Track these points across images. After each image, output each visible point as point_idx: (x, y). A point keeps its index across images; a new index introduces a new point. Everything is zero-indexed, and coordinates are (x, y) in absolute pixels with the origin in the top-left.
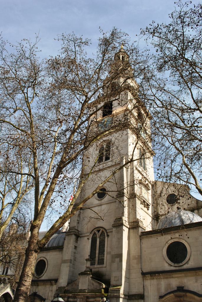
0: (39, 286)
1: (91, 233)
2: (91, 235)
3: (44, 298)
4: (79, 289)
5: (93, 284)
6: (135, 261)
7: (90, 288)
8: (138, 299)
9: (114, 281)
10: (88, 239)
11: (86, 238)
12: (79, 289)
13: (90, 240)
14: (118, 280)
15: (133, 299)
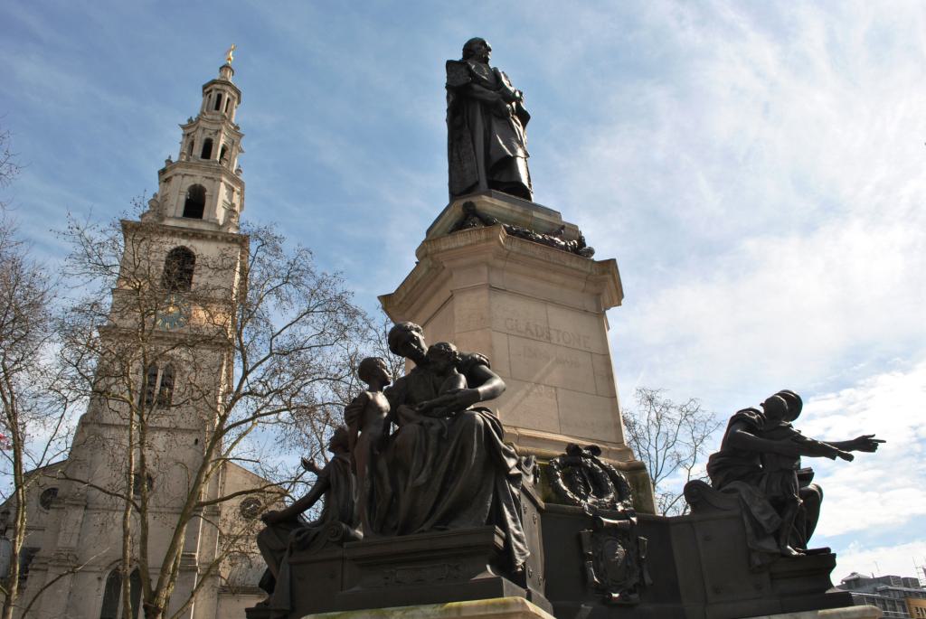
1: (108, 568)
2: (109, 572)
10: (100, 579)
11: (93, 577)
13: (104, 583)
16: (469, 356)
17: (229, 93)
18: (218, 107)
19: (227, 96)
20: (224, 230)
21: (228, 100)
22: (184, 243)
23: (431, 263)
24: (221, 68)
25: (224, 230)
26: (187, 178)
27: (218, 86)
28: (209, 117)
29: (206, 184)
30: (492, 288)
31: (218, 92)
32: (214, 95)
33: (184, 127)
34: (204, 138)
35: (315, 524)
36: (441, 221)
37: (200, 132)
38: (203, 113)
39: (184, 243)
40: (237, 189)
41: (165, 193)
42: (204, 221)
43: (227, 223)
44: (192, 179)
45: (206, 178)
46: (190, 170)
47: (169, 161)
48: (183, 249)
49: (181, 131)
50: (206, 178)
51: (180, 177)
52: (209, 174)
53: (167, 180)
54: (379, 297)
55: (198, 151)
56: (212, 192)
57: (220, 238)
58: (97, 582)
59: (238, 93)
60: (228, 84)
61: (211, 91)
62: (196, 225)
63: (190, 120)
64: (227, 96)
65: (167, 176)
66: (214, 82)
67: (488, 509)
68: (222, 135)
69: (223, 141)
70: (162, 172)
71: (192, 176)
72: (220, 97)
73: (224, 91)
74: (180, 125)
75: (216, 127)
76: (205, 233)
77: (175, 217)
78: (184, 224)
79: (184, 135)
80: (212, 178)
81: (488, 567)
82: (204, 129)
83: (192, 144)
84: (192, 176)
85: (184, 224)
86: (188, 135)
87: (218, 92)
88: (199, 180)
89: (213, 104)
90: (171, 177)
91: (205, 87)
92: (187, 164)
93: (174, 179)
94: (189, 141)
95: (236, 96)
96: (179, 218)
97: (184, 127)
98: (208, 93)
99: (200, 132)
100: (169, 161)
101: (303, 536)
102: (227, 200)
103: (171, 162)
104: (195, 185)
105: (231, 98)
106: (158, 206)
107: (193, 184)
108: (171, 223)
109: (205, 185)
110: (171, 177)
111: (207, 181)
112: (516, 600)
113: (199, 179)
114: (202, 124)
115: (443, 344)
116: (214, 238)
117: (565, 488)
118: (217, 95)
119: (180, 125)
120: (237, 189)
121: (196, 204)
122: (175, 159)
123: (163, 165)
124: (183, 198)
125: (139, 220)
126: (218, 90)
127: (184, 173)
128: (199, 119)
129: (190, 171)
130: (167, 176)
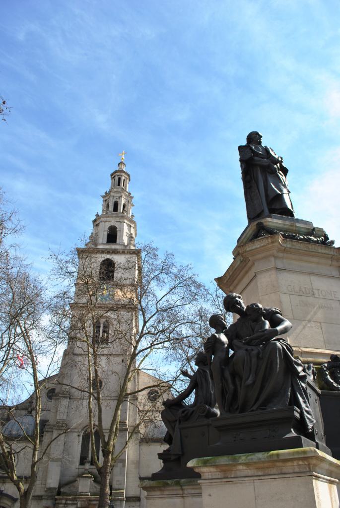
0: (6, 484)
1: (82, 430)
2: (83, 432)
3: (15, 497)
4: (79, 491)
5: (96, 487)
6: (133, 466)
7: (91, 491)
8: (136, 501)
9: (117, 484)
10: (79, 435)
11: (75, 434)
12: (79, 491)
13: (81, 438)
14: (121, 484)
15: (130, 501)
16: (269, 309)
17: (124, 177)
18: (119, 185)
19: (123, 178)
20: (128, 248)
21: (124, 180)
22: (108, 256)
23: (242, 258)
25: (128, 248)
26: (107, 223)
27: (118, 174)
28: (115, 190)
29: (117, 225)
30: (278, 269)
32: (117, 178)
33: (103, 197)
34: (114, 201)
35: (192, 406)
36: (244, 235)
37: (111, 198)
38: (112, 188)
39: (108, 256)
40: (133, 225)
41: (97, 231)
42: (119, 244)
43: (129, 244)
44: (110, 223)
45: (117, 221)
46: (108, 218)
47: (97, 215)
48: (108, 260)
49: (102, 199)
50: (117, 221)
51: (103, 223)
52: (118, 220)
53: (97, 225)
54: (215, 279)
55: (111, 208)
56: (120, 228)
57: (126, 252)
58: (77, 437)
59: (129, 175)
60: (123, 172)
61: (115, 176)
62: (114, 247)
63: (106, 193)
64: (123, 178)
65: (97, 223)
66: (116, 172)
67: (289, 396)
68: (123, 199)
69: (123, 201)
70: (95, 221)
71: (109, 221)
72: (119, 179)
73: (122, 176)
75: (119, 195)
77: (103, 244)
78: (108, 247)
79: (103, 201)
80: (119, 221)
81: (292, 430)
82: (113, 197)
83: (108, 205)
84: (109, 221)
85: (108, 247)
86: (106, 200)
88: (113, 223)
89: (117, 183)
90: (99, 224)
91: (112, 175)
92: (106, 216)
93: (101, 224)
94: (106, 204)
95: (128, 177)
96: (105, 244)
97: (103, 197)
98: (114, 177)
99: (111, 198)
100: (97, 215)
101: (185, 413)
102: (128, 232)
103: (98, 215)
104: (111, 226)
105: (125, 179)
106: (94, 239)
107: (110, 225)
108: (101, 247)
109: (116, 225)
110: (99, 224)
111: (117, 223)
112: (310, 449)
113: (113, 222)
114: (112, 194)
115: (254, 304)
116: (123, 253)
117: (332, 381)
118: (118, 178)
120: (133, 225)
121: (112, 236)
122: (100, 214)
123: (94, 218)
124: (106, 234)
125: (84, 247)
126: (118, 175)
128: (110, 192)
129: (108, 219)
130: (97, 223)
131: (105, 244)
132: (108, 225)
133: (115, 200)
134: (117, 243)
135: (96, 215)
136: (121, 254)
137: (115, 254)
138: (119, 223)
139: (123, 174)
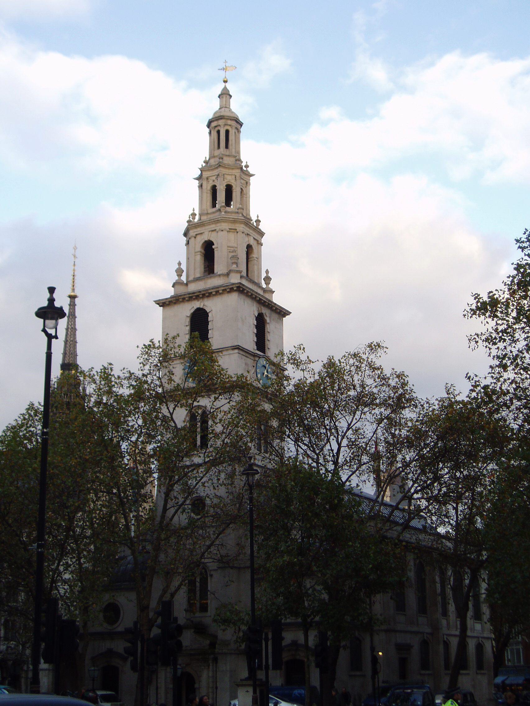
21: (227, 132)
22: (197, 304)
24: (219, 97)
26: (198, 237)
27: (213, 124)
29: (213, 237)
31: (217, 129)
32: (214, 133)
34: (209, 188)
46: (199, 229)
49: (197, 183)
52: (213, 227)
71: (202, 233)
72: (218, 132)
73: (219, 125)
74: (194, 179)
76: (210, 291)
79: (199, 187)
82: (207, 179)
87: (217, 129)
88: (205, 237)
95: (233, 123)
96: (197, 280)
107: (203, 241)
119: (194, 179)
126: (216, 127)
127: (194, 234)
129: (199, 230)
131: (197, 280)
132: (200, 240)
133: (211, 184)
134: (215, 272)
135: (187, 222)
136: (214, 295)
137: (208, 297)
138: (214, 233)
139: (221, 122)
